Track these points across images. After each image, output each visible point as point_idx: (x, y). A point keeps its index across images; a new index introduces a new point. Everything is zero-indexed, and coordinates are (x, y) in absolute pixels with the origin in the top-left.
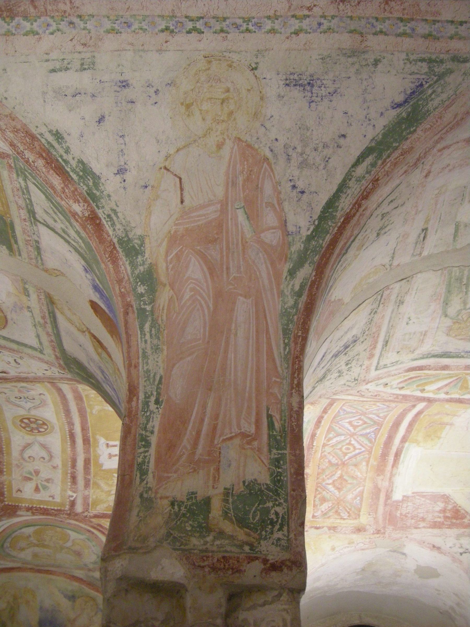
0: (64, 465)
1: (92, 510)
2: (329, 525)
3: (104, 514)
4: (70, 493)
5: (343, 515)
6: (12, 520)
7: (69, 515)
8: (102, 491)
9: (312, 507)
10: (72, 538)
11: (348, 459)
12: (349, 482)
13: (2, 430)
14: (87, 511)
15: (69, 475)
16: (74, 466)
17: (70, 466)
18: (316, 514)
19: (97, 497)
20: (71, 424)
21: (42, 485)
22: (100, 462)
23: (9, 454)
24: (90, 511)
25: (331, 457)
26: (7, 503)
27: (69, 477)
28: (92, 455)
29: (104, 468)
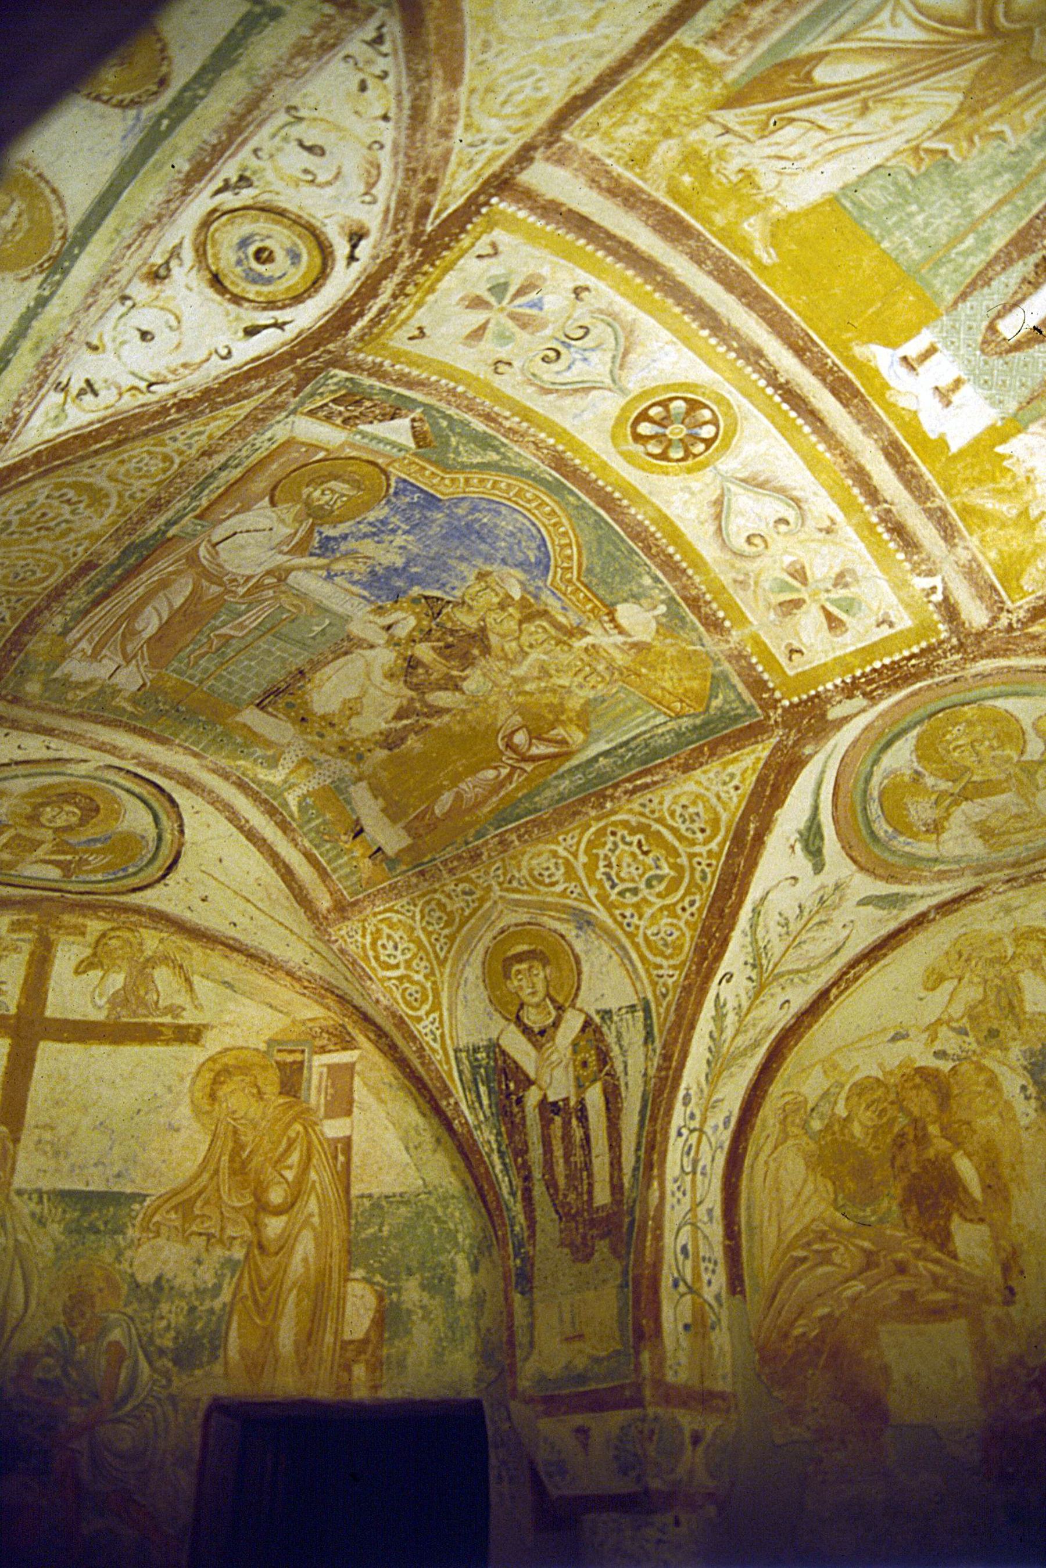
0: (848, 507)
6: (832, 742)
7: (961, 647)
8: (1003, 525)
10: (1027, 723)
13: (625, 502)
14: (1001, 609)
15: (880, 529)
16: (873, 495)
17: (861, 500)
19: (1000, 552)
20: (753, 354)
21: (833, 602)
22: (932, 436)
23: (698, 563)
24: (1009, 605)
26: (786, 703)
27: (886, 536)
28: (891, 425)
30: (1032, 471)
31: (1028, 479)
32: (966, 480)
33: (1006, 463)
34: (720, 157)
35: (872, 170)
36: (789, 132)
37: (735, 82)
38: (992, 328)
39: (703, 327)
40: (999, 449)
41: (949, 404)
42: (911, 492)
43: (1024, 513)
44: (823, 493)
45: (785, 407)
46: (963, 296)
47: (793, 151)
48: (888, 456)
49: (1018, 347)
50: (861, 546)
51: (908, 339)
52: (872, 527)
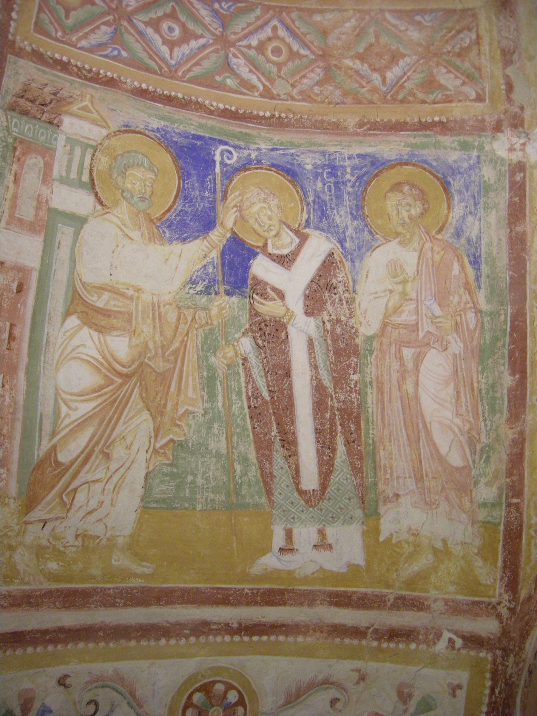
1: (494, 597)
2: (500, 65)
3: (505, 567)
4: (441, 645)
5: (468, 41)
7: (506, 651)
8: (435, 569)
9: (453, 104)
11: (309, 48)
12: (373, 40)
14: (494, 607)
15: (385, 645)
17: (356, 642)
18: (473, 95)
22: (344, 570)
24: (494, 600)
25: (305, 81)
27: (392, 645)
28: (317, 588)
29: (359, 559)
30: (410, 529)
31: (413, 534)
32: (388, 570)
33: (394, 541)
34: (56, 538)
35: (146, 479)
36: (81, 497)
37: (20, 493)
38: (302, 493)
39: (158, 639)
40: (382, 538)
41: (330, 547)
42: (372, 608)
43: (435, 552)
44: (333, 661)
45: (255, 638)
46: (269, 493)
47: (93, 504)
48: (337, 604)
49: (324, 487)
50: (388, 665)
51: (270, 538)
52: (379, 649)
